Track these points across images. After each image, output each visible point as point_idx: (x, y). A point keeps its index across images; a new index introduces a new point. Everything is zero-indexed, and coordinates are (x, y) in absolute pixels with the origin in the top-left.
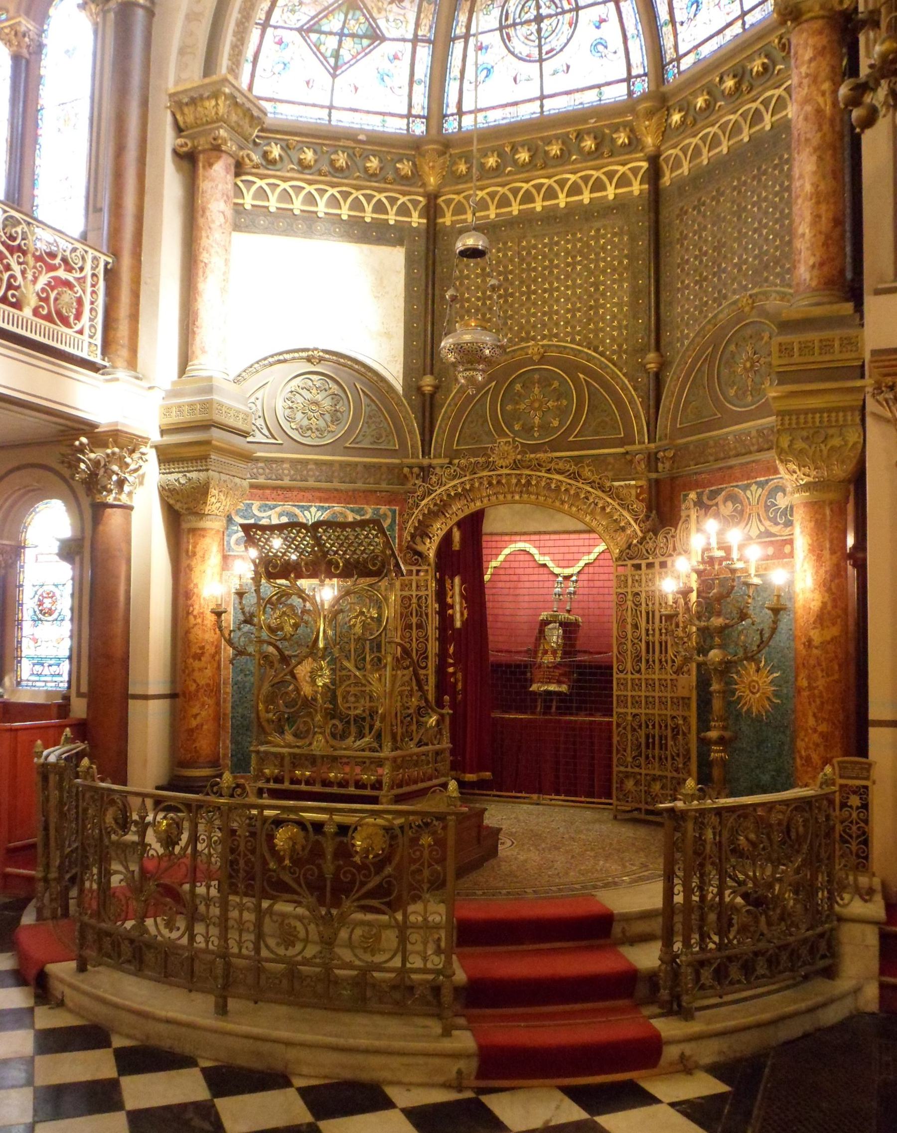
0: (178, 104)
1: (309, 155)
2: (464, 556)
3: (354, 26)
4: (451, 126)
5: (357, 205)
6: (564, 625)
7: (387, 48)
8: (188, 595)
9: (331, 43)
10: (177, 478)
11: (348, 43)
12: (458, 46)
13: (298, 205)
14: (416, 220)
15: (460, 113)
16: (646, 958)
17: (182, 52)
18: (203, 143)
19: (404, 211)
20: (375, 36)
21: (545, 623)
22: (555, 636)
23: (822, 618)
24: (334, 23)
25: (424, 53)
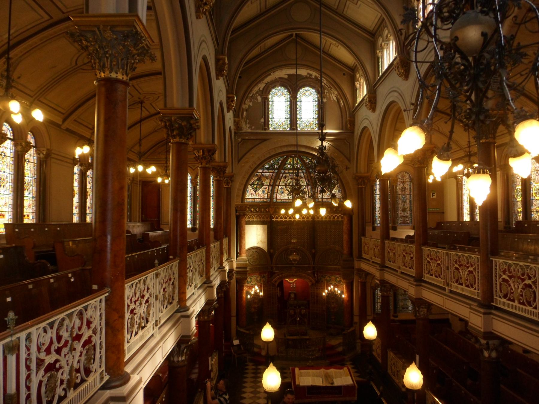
0: (237, 207)
1: (252, 209)
2: (281, 285)
3: (259, 183)
4: (275, 201)
5: (260, 218)
6: (295, 293)
7: (264, 187)
8: (241, 297)
9: (255, 186)
10: (239, 276)
11: (258, 186)
12: (277, 187)
13: (251, 219)
14: (269, 219)
15: (277, 199)
16: (340, 349)
17: (237, 196)
18: (242, 214)
19: (267, 218)
20: (263, 185)
21: (290, 293)
22: (292, 296)
23: (348, 301)
24: (256, 183)
25: (270, 187)
